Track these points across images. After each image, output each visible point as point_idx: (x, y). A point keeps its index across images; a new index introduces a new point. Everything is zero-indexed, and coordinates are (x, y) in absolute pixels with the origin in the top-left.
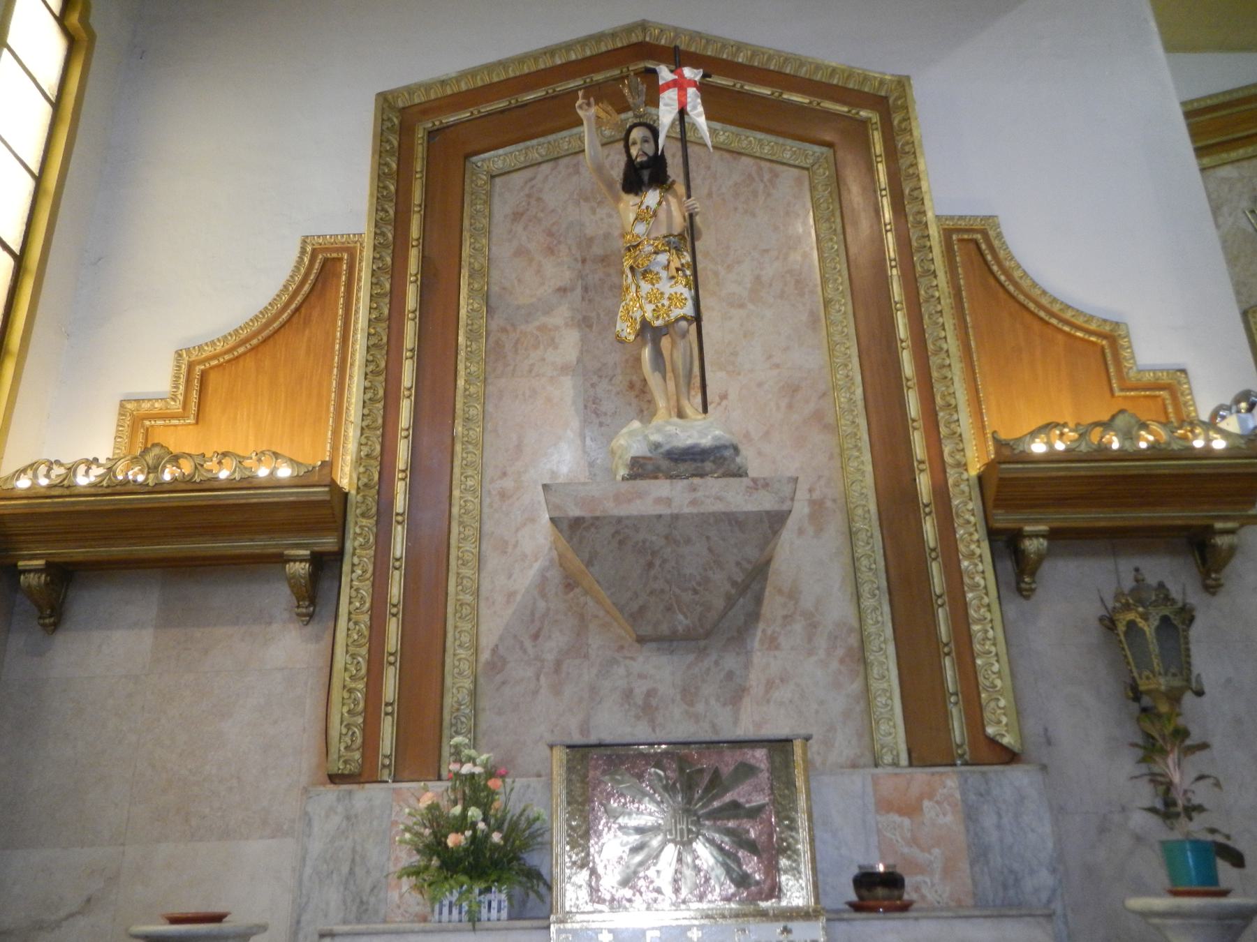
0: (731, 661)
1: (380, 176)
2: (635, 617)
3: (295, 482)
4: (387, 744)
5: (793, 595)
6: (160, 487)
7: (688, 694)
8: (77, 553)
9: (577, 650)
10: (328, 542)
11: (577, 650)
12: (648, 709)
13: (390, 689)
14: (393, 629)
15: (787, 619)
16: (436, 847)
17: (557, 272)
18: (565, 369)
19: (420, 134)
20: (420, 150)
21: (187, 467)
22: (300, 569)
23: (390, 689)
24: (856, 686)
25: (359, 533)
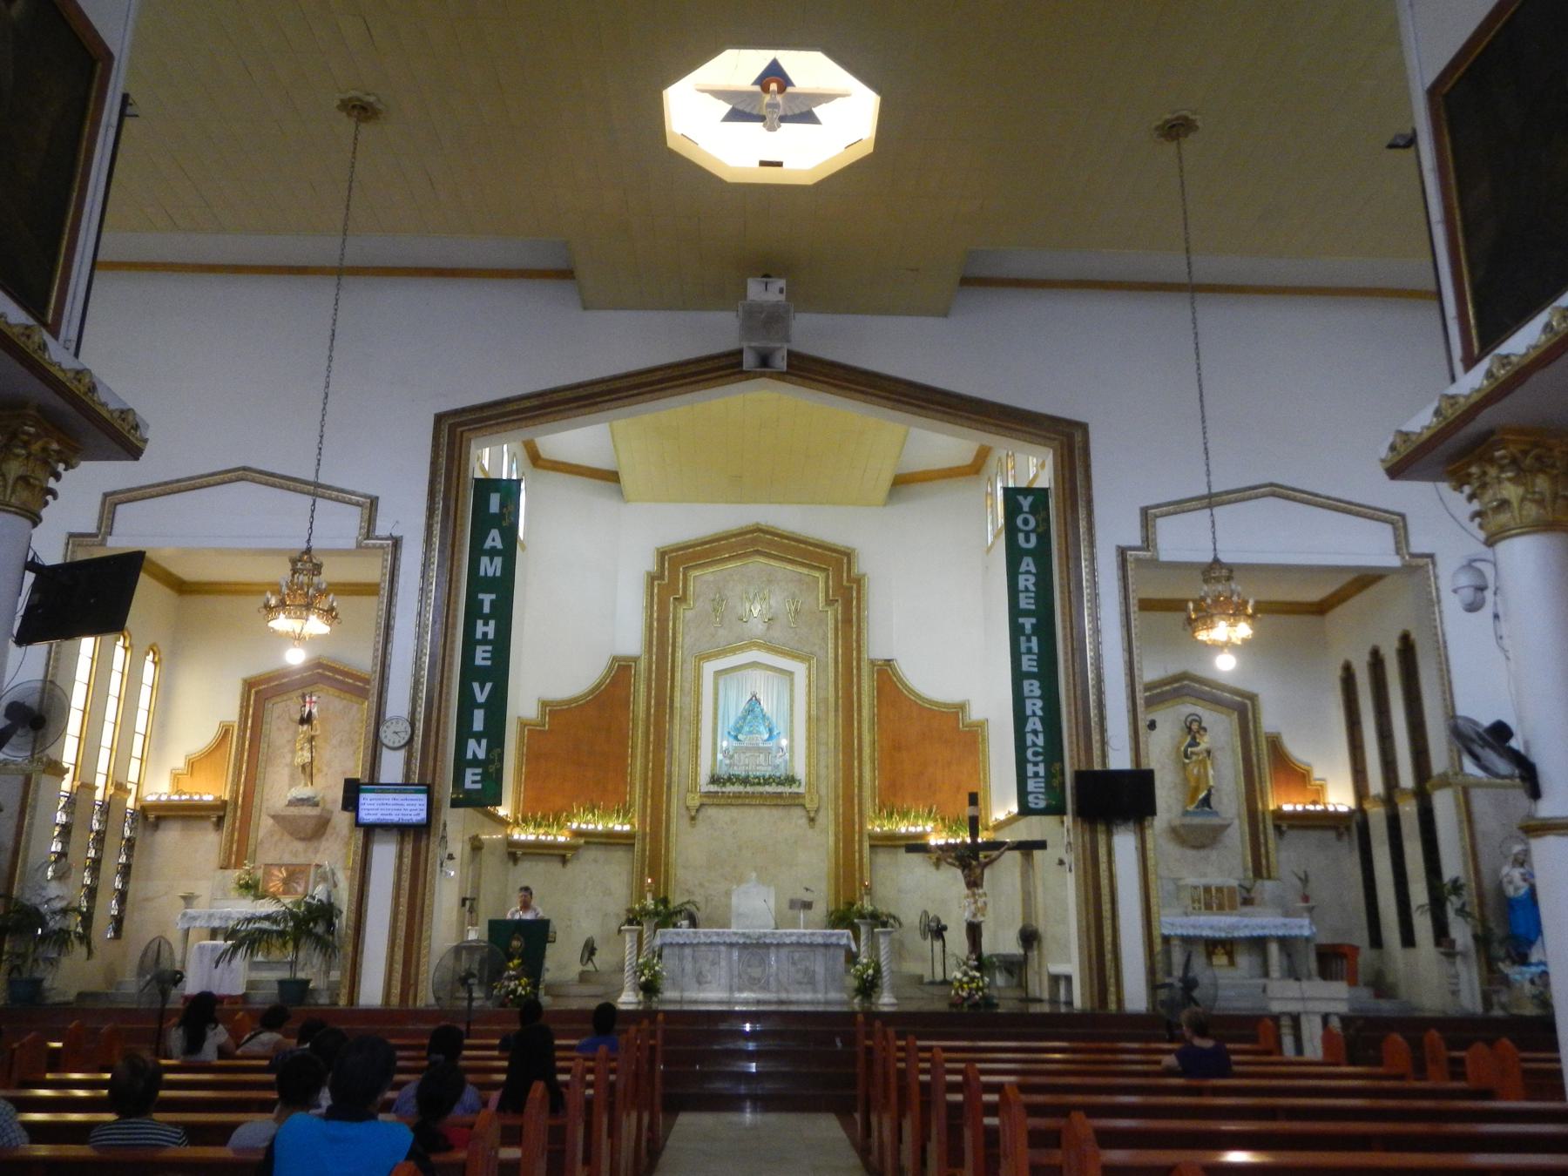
0: (316, 844)
1: (242, 707)
2: (291, 834)
3: (215, 799)
4: (233, 861)
5: (334, 828)
6: (181, 800)
7: (306, 851)
8: (162, 813)
9: (281, 840)
10: (221, 813)
11: (281, 840)
12: (296, 854)
13: (234, 848)
14: (236, 834)
15: (332, 835)
16: (238, 883)
17: (287, 736)
18: (287, 765)
19: (253, 691)
20: (252, 698)
21: (187, 797)
22: (214, 819)
23: (234, 848)
24: (344, 851)
25: (229, 808)
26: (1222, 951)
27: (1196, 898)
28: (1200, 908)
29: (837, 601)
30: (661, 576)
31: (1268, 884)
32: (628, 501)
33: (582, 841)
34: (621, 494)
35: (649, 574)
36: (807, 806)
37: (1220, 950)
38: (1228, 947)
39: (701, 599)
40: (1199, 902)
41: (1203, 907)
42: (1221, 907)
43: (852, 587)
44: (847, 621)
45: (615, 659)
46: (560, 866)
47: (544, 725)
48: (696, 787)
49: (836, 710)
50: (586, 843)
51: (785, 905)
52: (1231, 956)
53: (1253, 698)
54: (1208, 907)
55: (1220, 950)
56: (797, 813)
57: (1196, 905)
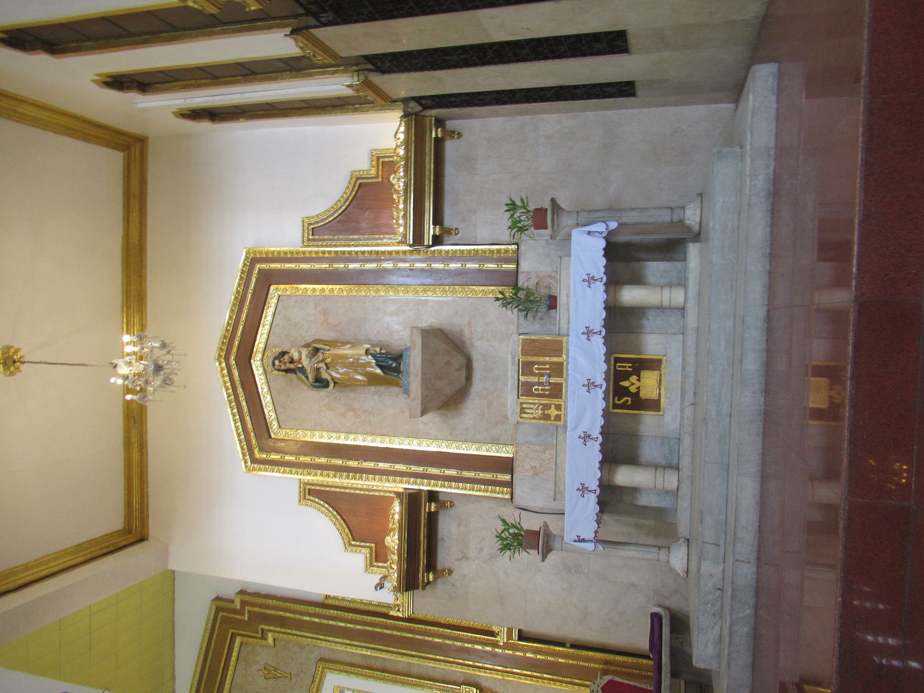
26: (634, 378)
27: (540, 412)
28: (558, 407)
29: (262, 629)
31: (524, 266)
37: (631, 383)
38: (628, 367)
40: (548, 407)
41: (556, 401)
42: (558, 369)
43: (249, 612)
44: (283, 622)
52: (641, 365)
53: (253, 261)
54: (556, 391)
55: (631, 383)
57: (553, 412)
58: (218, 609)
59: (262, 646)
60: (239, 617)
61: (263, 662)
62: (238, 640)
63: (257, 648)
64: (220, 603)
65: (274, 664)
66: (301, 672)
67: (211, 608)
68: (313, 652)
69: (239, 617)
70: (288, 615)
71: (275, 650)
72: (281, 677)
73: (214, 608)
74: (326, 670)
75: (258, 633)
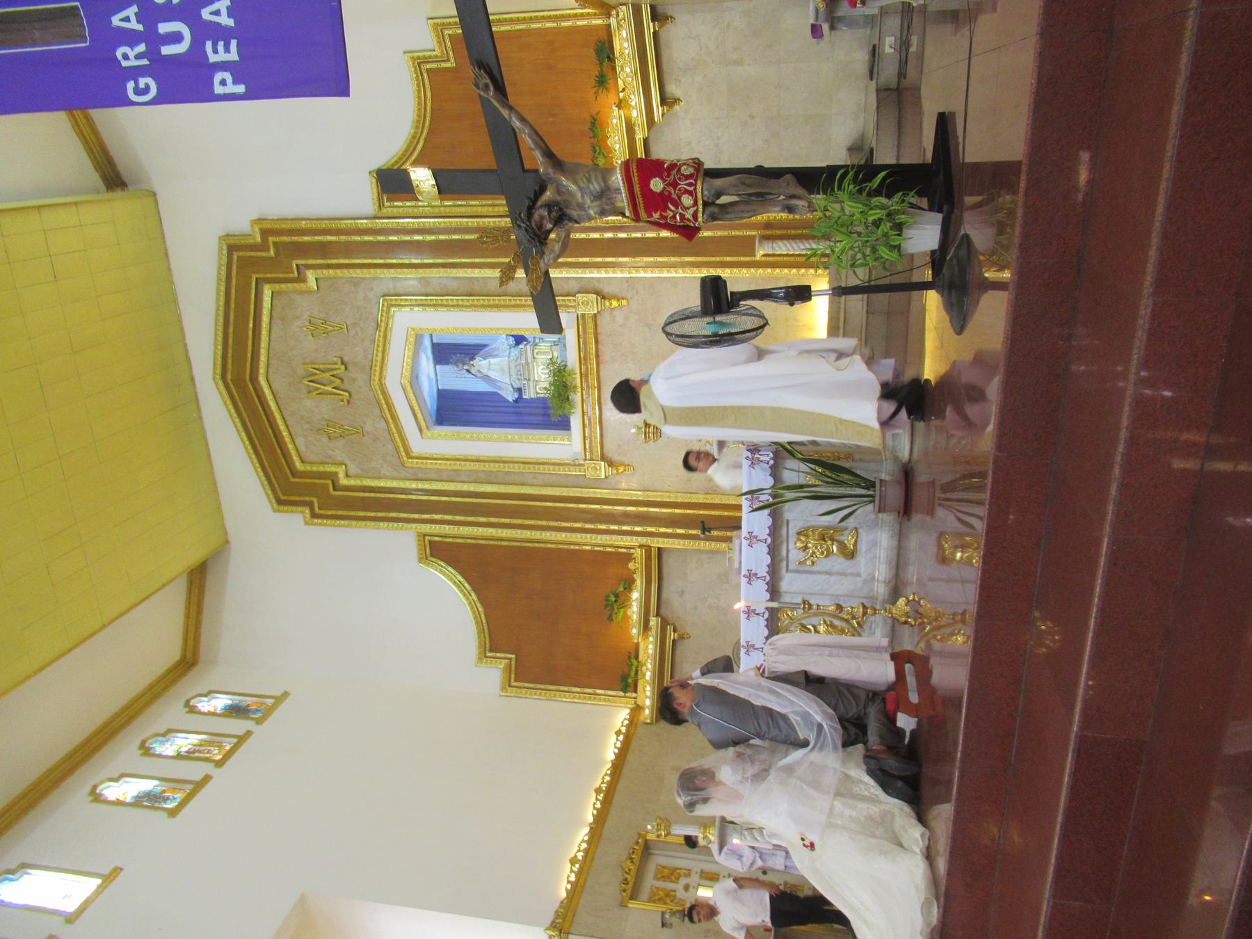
29: (297, 265)
30: (310, 505)
32: (227, 542)
33: (653, 621)
34: (223, 548)
35: (306, 523)
36: (596, 312)
39: (330, 453)
43: (275, 244)
44: (323, 250)
45: (423, 559)
46: (686, 641)
47: (510, 659)
48: (580, 465)
49: (453, 266)
50: (658, 614)
51: (702, 520)
56: (604, 321)
58: (232, 249)
59: (301, 293)
60: (263, 254)
61: (306, 316)
62: (267, 291)
63: (295, 297)
64: (232, 241)
65: (322, 316)
66: (360, 320)
67: (221, 249)
68: (372, 289)
69: (263, 254)
70: (330, 238)
71: (319, 295)
72: (334, 330)
73: (225, 247)
74: (393, 309)
75: (293, 273)
